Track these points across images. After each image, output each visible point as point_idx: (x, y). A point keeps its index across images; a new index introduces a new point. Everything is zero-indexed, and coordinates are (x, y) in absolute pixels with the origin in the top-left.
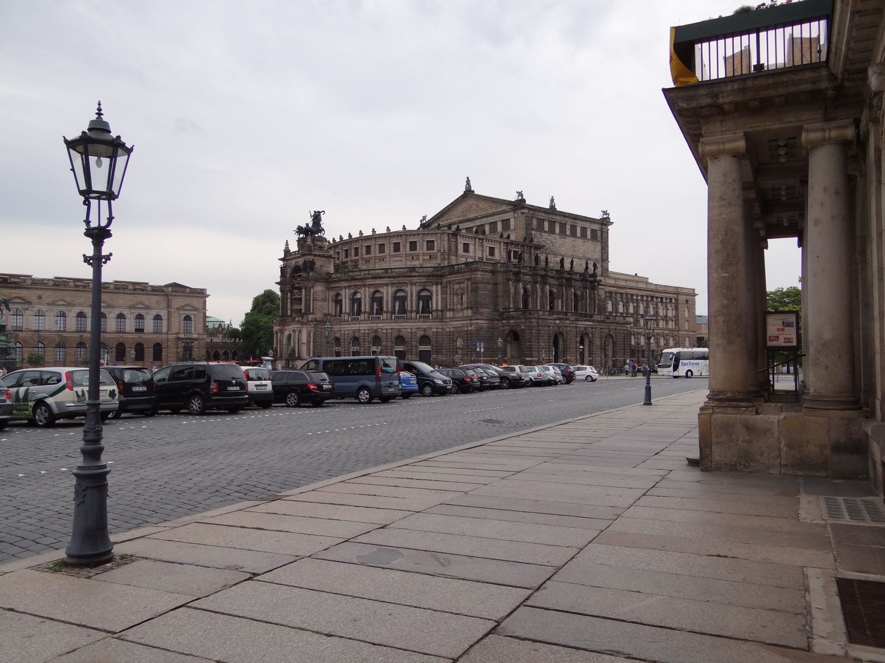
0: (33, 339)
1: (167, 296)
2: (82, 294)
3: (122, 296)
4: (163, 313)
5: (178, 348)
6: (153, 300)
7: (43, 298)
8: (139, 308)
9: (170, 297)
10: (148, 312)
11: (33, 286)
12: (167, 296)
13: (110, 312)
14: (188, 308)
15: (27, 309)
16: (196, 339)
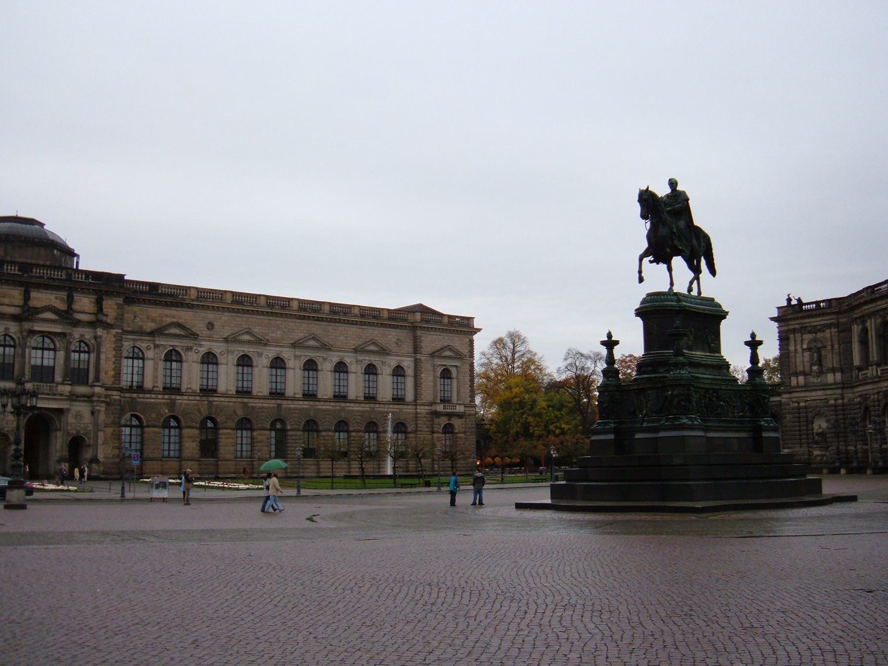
0: (199, 410)
1: (414, 328)
2: (279, 321)
3: (342, 327)
4: (408, 364)
5: (433, 432)
6: (390, 337)
7: (216, 327)
8: (372, 352)
9: (419, 333)
10: (384, 360)
11: (201, 301)
12: (414, 328)
13: (325, 359)
14: (448, 353)
15: (189, 349)
16: (460, 416)
